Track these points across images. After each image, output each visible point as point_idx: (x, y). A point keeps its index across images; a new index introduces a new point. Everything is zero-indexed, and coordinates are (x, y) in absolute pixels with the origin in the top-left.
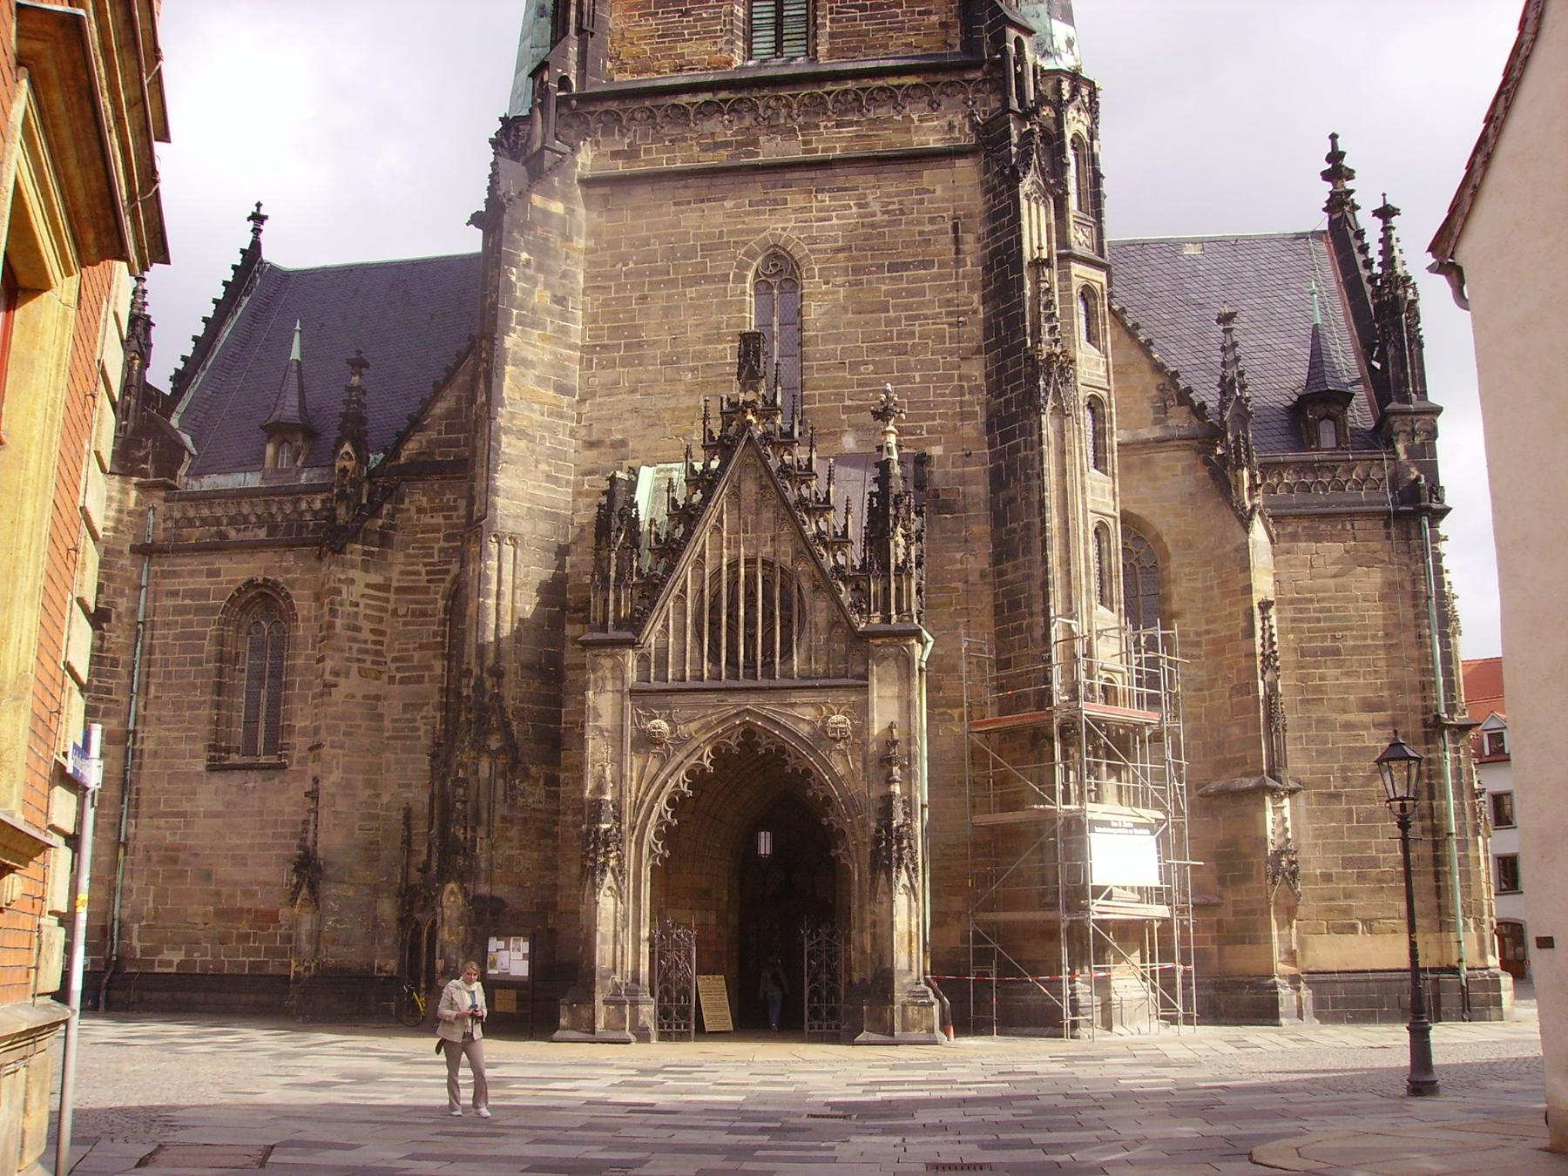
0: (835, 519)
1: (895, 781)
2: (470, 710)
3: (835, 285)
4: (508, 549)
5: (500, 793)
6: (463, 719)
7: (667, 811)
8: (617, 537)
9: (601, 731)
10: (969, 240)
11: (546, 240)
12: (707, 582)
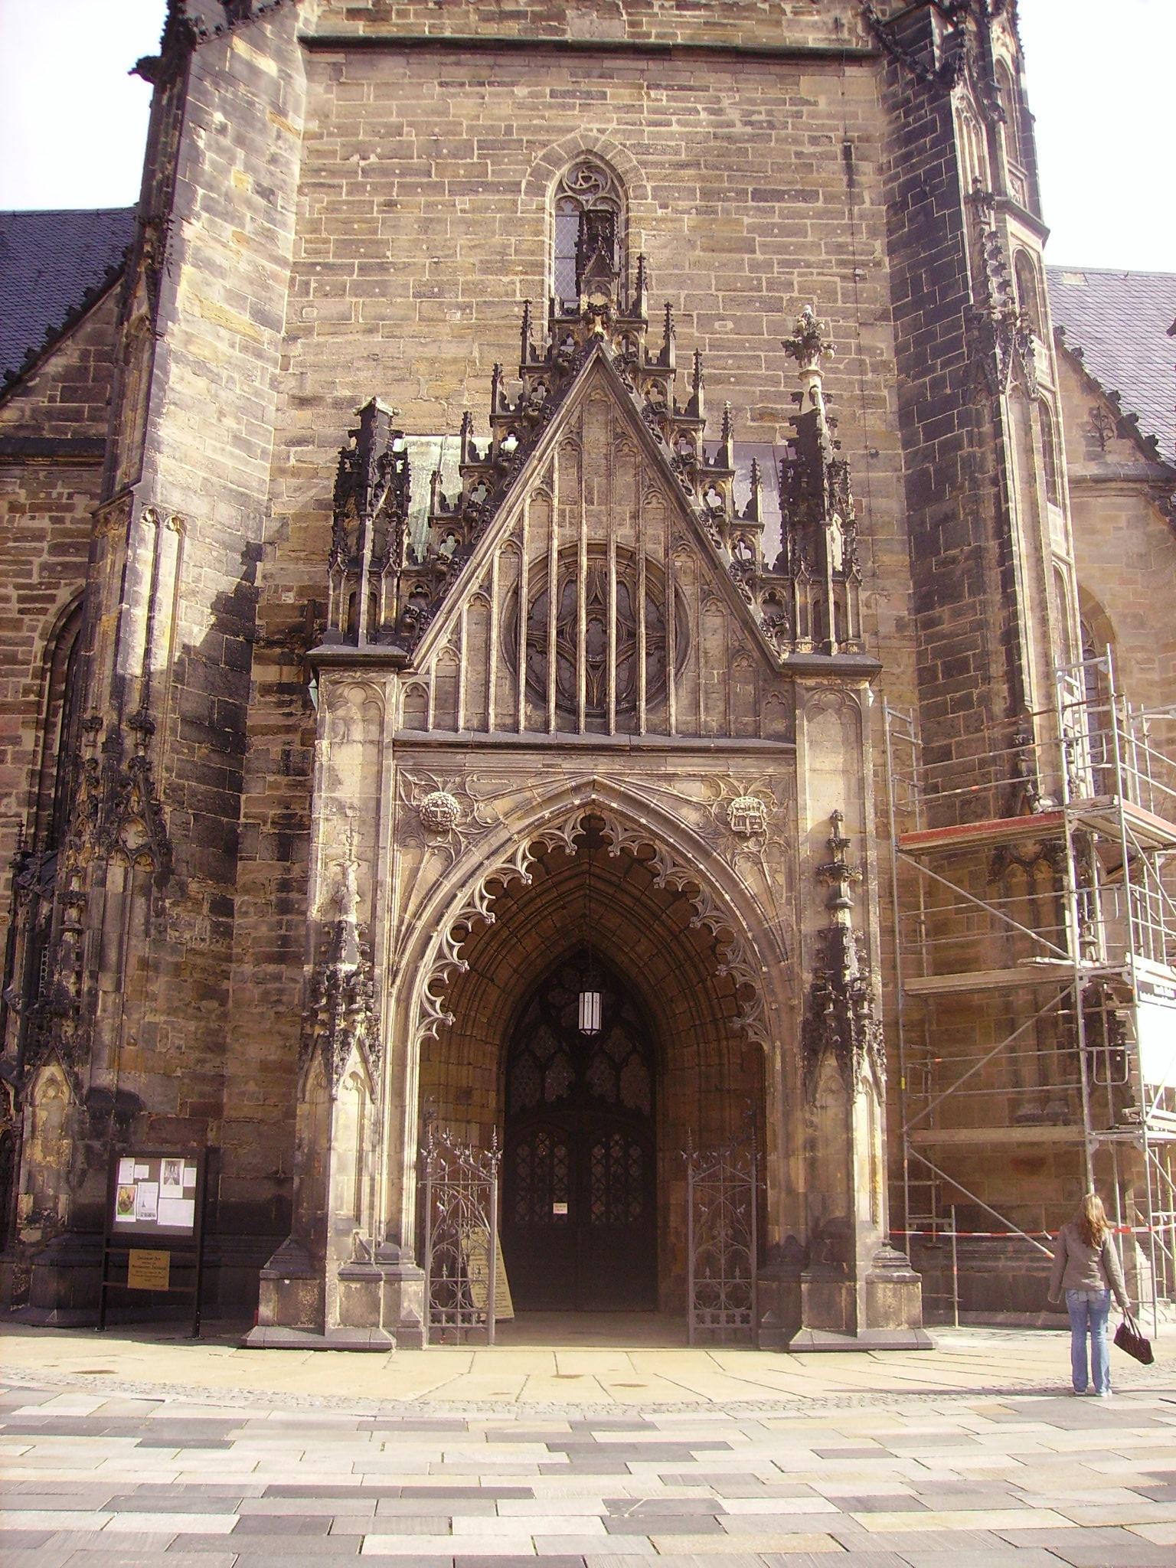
0: (738, 491)
1: (844, 906)
2: (95, 783)
3: (676, 211)
4: (170, 538)
5: (139, 919)
6: (82, 796)
7: (451, 947)
8: (376, 496)
9: (341, 807)
10: (867, 174)
11: (251, 104)
12: (525, 575)
